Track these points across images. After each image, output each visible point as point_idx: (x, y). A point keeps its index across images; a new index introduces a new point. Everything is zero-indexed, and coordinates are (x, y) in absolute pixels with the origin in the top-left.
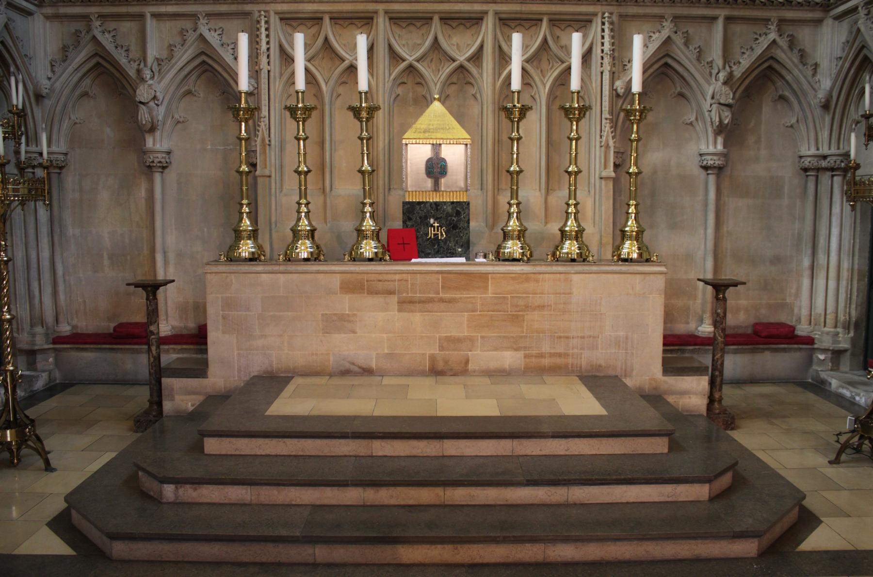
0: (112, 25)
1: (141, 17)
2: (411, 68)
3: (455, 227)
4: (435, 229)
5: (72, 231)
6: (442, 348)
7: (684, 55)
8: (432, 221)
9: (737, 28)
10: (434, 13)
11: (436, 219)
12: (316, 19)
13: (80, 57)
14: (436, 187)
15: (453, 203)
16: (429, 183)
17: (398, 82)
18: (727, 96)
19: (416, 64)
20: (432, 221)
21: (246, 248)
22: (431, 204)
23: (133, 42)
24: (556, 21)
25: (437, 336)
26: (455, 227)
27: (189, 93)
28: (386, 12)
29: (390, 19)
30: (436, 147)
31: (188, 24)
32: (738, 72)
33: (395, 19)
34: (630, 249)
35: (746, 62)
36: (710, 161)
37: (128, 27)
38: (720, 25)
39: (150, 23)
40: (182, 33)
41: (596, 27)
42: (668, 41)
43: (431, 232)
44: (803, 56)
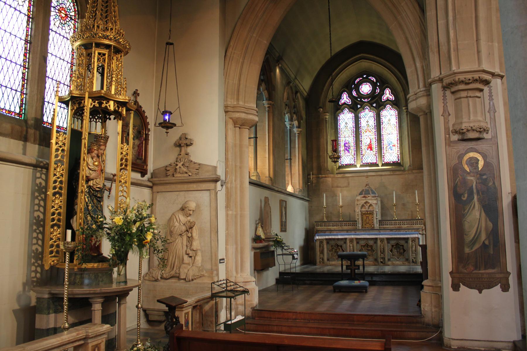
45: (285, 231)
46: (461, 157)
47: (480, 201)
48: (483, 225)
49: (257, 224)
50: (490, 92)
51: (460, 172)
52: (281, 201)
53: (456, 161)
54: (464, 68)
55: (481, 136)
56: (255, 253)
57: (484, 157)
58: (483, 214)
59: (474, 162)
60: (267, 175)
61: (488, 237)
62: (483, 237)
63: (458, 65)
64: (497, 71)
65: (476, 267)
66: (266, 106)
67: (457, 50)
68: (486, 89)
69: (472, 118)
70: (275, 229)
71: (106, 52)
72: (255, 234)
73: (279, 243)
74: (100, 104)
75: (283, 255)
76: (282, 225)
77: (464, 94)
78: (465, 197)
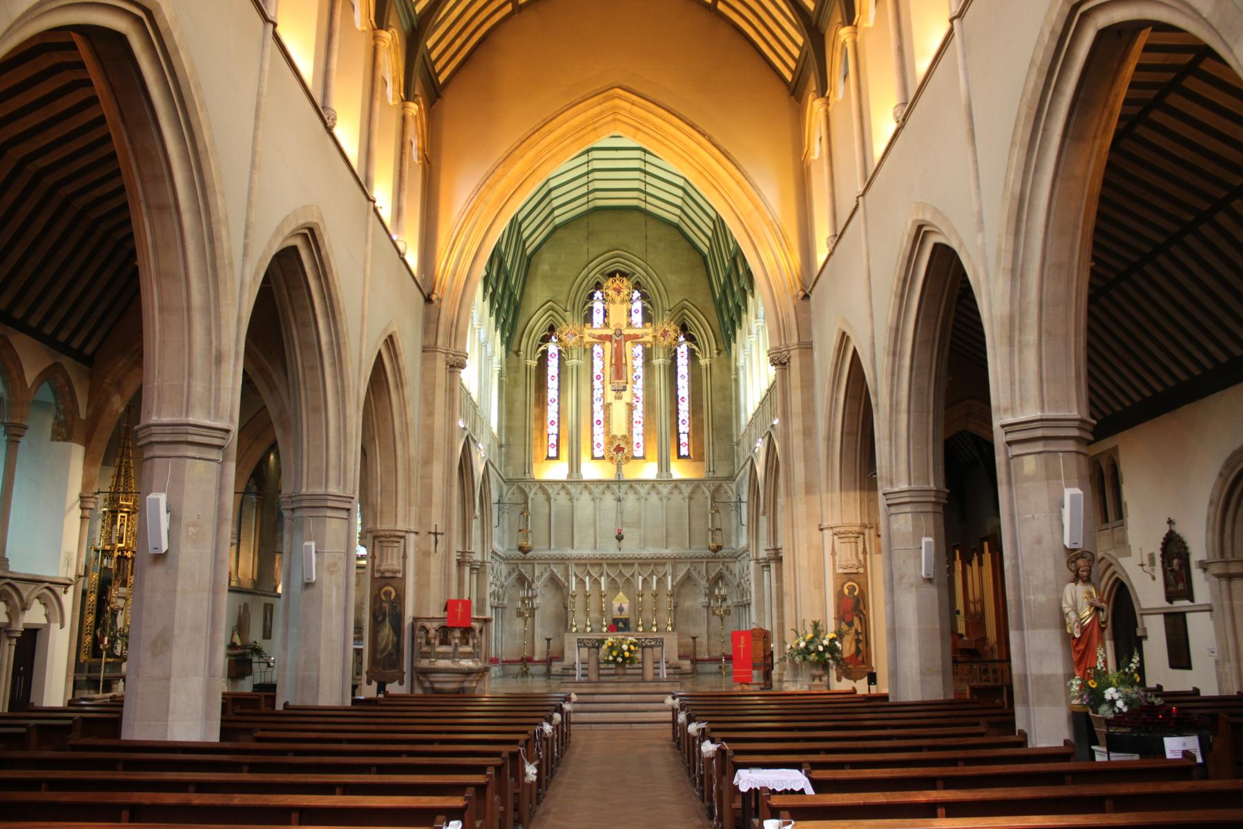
0: (524, 566)
1: (534, 564)
2: (613, 579)
4: (621, 625)
5: (507, 627)
7: (694, 574)
9: (710, 564)
12: (585, 565)
13: (514, 575)
14: (621, 614)
18: (707, 585)
21: (574, 629)
23: (530, 570)
24: (655, 564)
27: (546, 586)
31: (547, 566)
32: (711, 577)
33: (608, 565)
34: (670, 629)
35: (713, 574)
36: (705, 605)
37: (529, 567)
38: (704, 564)
39: (536, 566)
40: (545, 568)
41: (667, 566)
42: (689, 569)
44: (731, 572)
45: (269, 638)
46: (380, 589)
47: (389, 621)
48: (391, 639)
49: (233, 632)
50: (405, 543)
51: (378, 600)
52: (266, 605)
53: (377, 592)
54: (385, 527)
55: (394, 575)
56: (229, 661)
57: (396, 590)
58: (391, 631)
59: (388, 594)
60: (250, 577)
61: (393, 647)
62: (390, 647)
63: (381, 524)
64: (413, 528)
65: (384, 669)
66: (255, 501)
67: (381, 513)
68: (402, 541)
69: (389, 561)
70: (255, 635)
71: (125, 515)
72: (231, 641)
73: (258, 651)
74: (123, 553)
75: (259, 662)
76: (265, 631)
77: (385, 544)
78: (380, 619)
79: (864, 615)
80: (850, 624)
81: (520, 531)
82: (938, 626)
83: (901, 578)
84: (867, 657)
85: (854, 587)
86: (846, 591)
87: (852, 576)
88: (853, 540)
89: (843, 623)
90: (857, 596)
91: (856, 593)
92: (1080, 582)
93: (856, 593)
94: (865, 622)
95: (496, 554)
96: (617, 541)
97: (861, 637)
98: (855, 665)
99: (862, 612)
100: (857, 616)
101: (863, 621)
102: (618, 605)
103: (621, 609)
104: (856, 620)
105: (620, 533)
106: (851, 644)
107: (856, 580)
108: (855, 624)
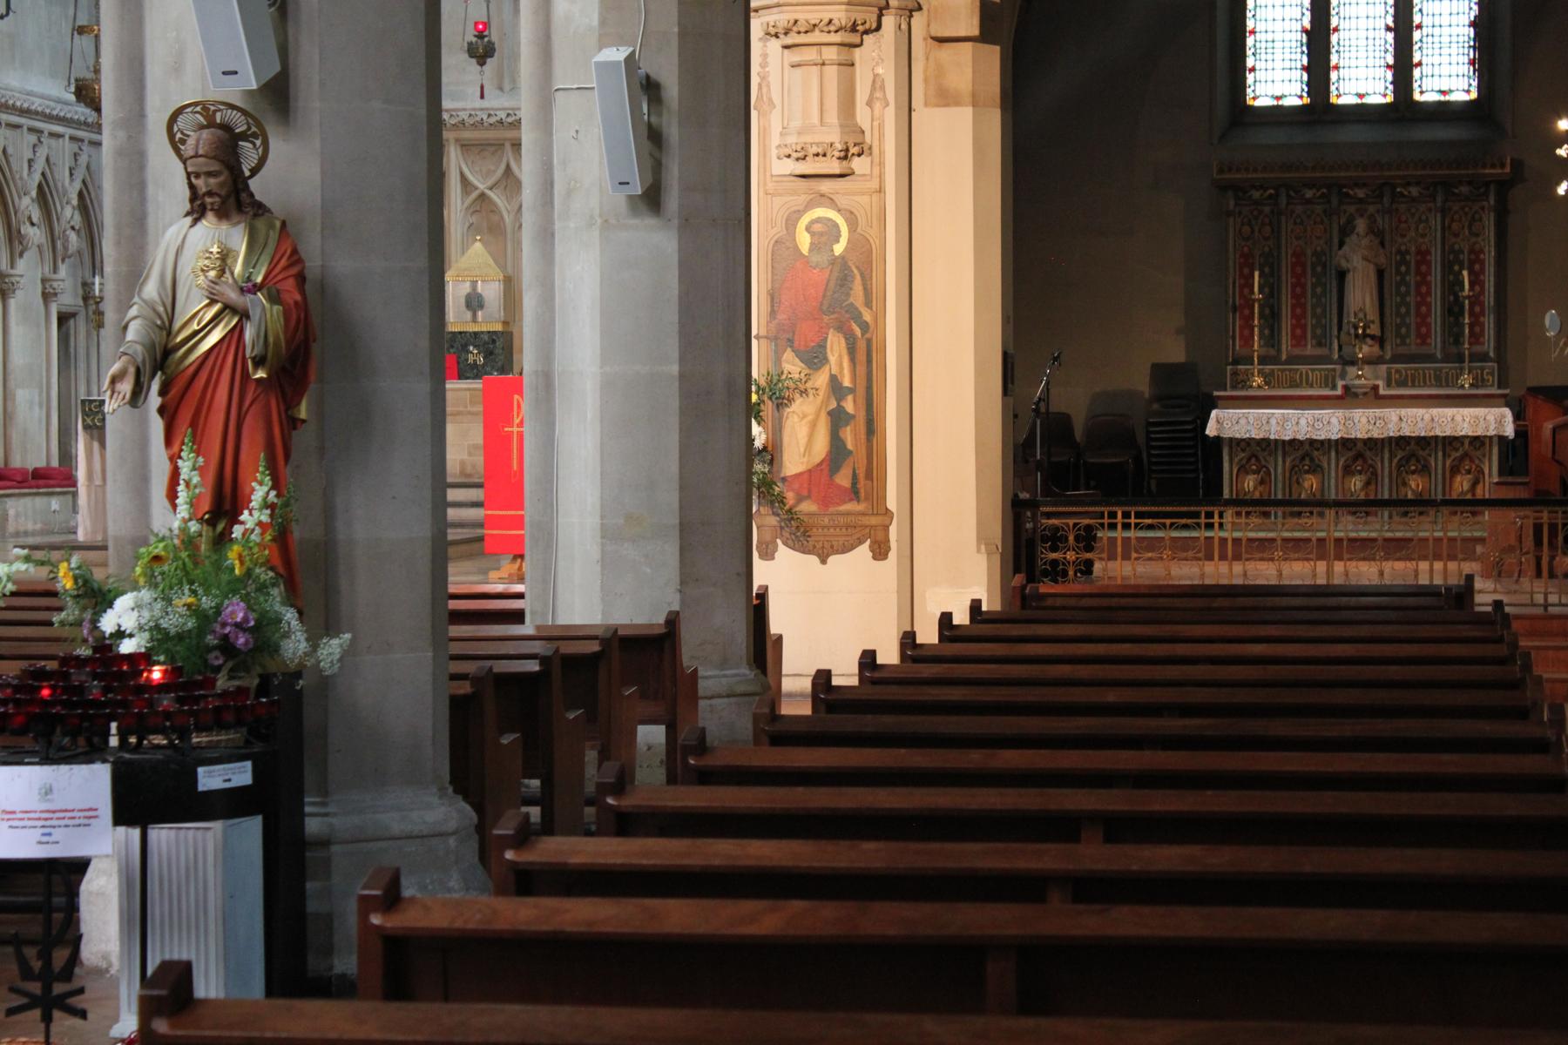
2: (482, 196)
3: (491, 353)
4: (475, 356)
6: (470, 454)
8: (471, 348)
10: (505, 139)
11: (475, 346)
15: (489, 332)
16: (469, 315)
17: (471, 210)
19: (489, 192)
20: (471, 348)
22: (470, 333)
25: (466, 443)
26: (491, 353)
28: (457, 140)
29: (462, 146)
30: (474, 283)
33: (465, 146)
43: (471, 359)
79: (865, 327)
80: (815, 358)
81: (81, 30)
82: (675, 369)
83: (569, 193)
84: (869, 476)
85: (836, 226)
86: (804, 241)
87: (826, 186)
88: (831, 54)
89: (789, 355)
90: (842, 257)
91: (839, 249)
92: (210, 216)
93: (839, 249)
94: (866, 354)
95: (24, 112)
96: (474, 61)
97: (849, 405)
98: (825, 502)
99: (857, 317)
100: (842, 328)
101: (862, 345)
102: (466, 288)
103: (474, 303)
104: (836, 348)
105: (480, 36)
106: (813, 426)
107: (842, 201)
108: (833, 359)
